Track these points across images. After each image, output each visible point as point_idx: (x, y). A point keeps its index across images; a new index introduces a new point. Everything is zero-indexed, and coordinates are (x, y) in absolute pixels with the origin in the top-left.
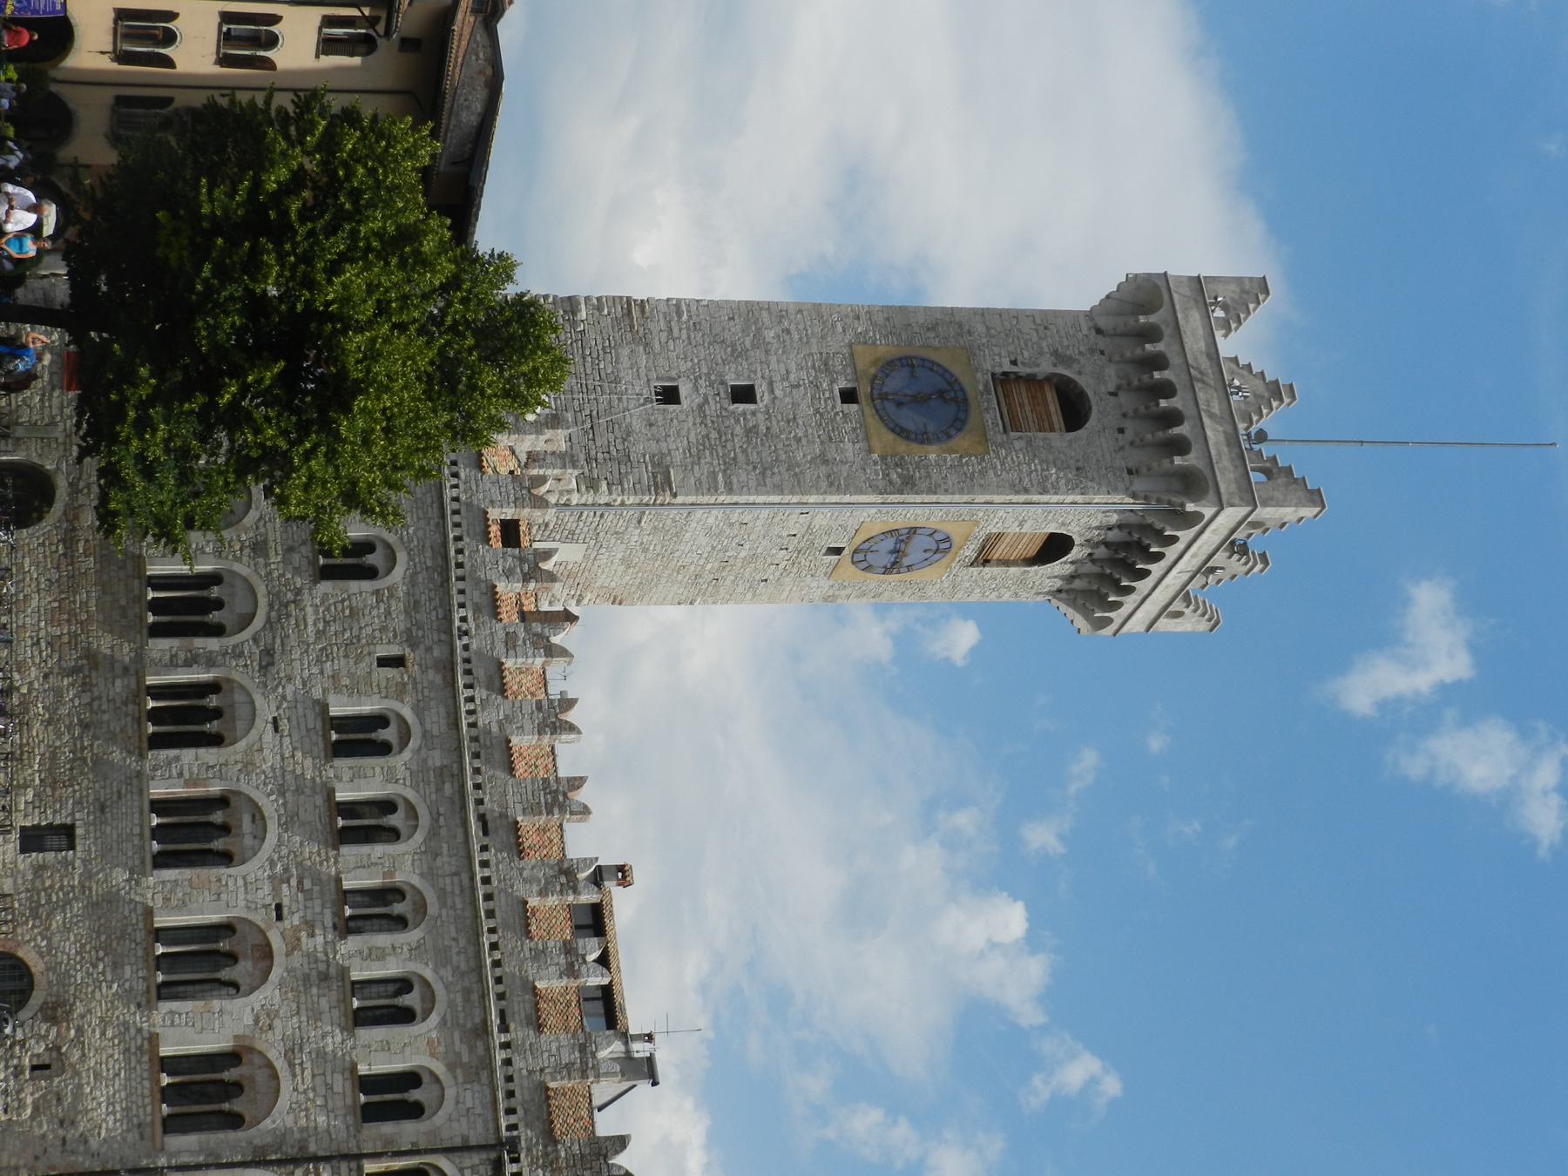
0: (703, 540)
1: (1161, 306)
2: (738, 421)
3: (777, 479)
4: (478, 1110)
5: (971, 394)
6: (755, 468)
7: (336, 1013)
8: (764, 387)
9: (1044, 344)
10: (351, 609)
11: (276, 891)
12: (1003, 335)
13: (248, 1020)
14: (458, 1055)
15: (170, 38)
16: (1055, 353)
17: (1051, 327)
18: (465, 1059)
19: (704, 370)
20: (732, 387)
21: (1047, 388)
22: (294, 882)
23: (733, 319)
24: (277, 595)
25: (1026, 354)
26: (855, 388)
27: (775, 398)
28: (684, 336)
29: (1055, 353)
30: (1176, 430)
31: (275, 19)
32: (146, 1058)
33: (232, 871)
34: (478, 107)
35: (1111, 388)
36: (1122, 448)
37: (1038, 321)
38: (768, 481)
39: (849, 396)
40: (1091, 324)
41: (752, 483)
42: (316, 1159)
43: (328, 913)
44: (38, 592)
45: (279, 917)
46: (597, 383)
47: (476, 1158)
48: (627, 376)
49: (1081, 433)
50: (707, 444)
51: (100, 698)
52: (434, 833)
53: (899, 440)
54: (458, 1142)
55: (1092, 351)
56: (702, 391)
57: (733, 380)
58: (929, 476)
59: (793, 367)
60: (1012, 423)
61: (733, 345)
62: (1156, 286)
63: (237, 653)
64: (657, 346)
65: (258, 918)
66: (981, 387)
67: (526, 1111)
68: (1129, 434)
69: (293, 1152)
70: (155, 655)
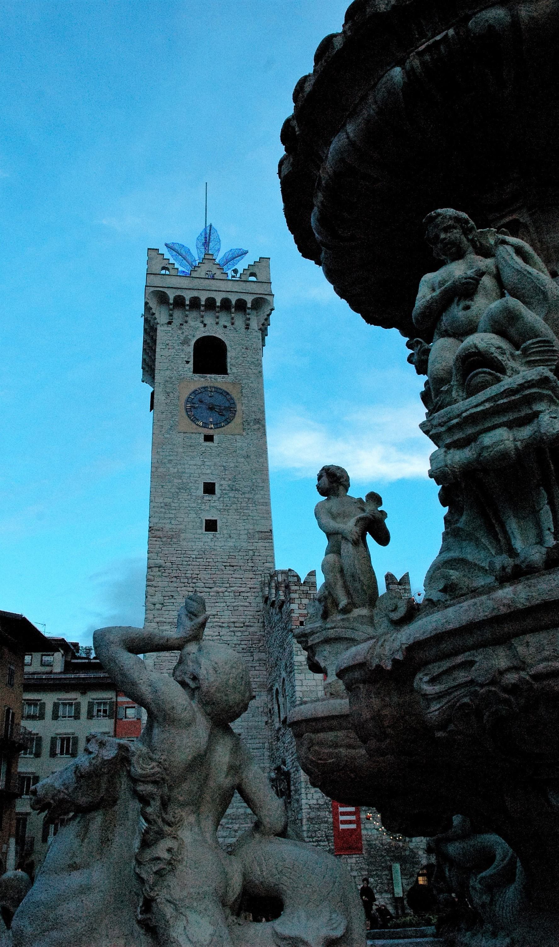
1: (164, 292)
2: (226, 494)
3: (259, 481)
6: (253, 490)
9: (177, 348)
12: (172, 364)
23: (162, 486)
25: (184, 356)
26: (205, 435)
28: (173, 512)
30: (233, 302)
36: (235, 329)
37: (164, 347)
38: (260, 485)
40: (166, 325)
46: (205, 560)
48: (199, 545)
50: (241, 510)
55: (180, 329)
56: (208, 508)
58: (254, 412)
59: (192, 462)
61: (179, 489)
62: (153, 292)
66: (202, 379)
68: (228, 324)
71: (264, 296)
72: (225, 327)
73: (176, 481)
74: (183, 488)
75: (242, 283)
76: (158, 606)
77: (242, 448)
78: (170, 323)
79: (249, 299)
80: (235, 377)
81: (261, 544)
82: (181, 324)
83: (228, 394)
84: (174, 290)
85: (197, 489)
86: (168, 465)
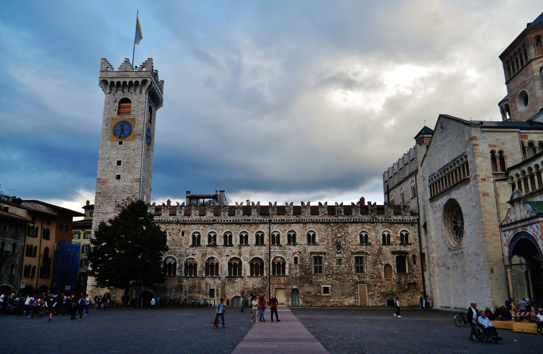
0: (145, 174)
2: (125, 165)
4: (263, 225)
5: (122, 120)
7: (246, 247)
8: (118, 158)
9: (112, 104)
10: (173, 240)
11: (224, 256)
13: (246, 261)
14: (254, 228)
15: (30, 266)
16: (114, 102)
17: (109, 102)
18: (255, 227)
19: (113, 170)
20: (117, 165)
21: (121, 105)
22: (223, 253)
24: (169, 253)
27: (120, 157)
28: (106, 172)
29: (114, 102)
30: (134, 83)
31: (28, 245)
32: (251, 278)
33: (220, 263)
34: (41, 206)
35: (122, 93)
39: (121, 143)
41: (138, 164)
42: (270, 252)
43: (228, 248)
44: (166, 294)
45: (229, 256)
47: (271, 227)
48: (113, 185)
49: (132, 100)
51: (187, 284)
52: (215, 229)
53: (131, 135)
54: (268, 229)
55: (114, 95)
56: (118, 170)
57: (116, 164)
58: (139, 131)
60: (129, 113)
61: (108, 164)
63: (179, 261)
64: (107, 178)
65: (229, 259)
66: (121, 118)
67: (264, 218)
68: (133, 92)
69: (268, 256)
70: (179, 275)
71: (147, 79)
72: (132, 93)
73: (107, 160)
74: (110, 163)
75: (138, 72)
76: (98, 207)
77: (132, 146)
78: (110, 93)
79: (140, 80)
80: (133, 116)
81: (135, 183)
82: (115, 93)
83: (130, 124)
84: (110, 79)
85: (115, 163)
86: (105, 154)
